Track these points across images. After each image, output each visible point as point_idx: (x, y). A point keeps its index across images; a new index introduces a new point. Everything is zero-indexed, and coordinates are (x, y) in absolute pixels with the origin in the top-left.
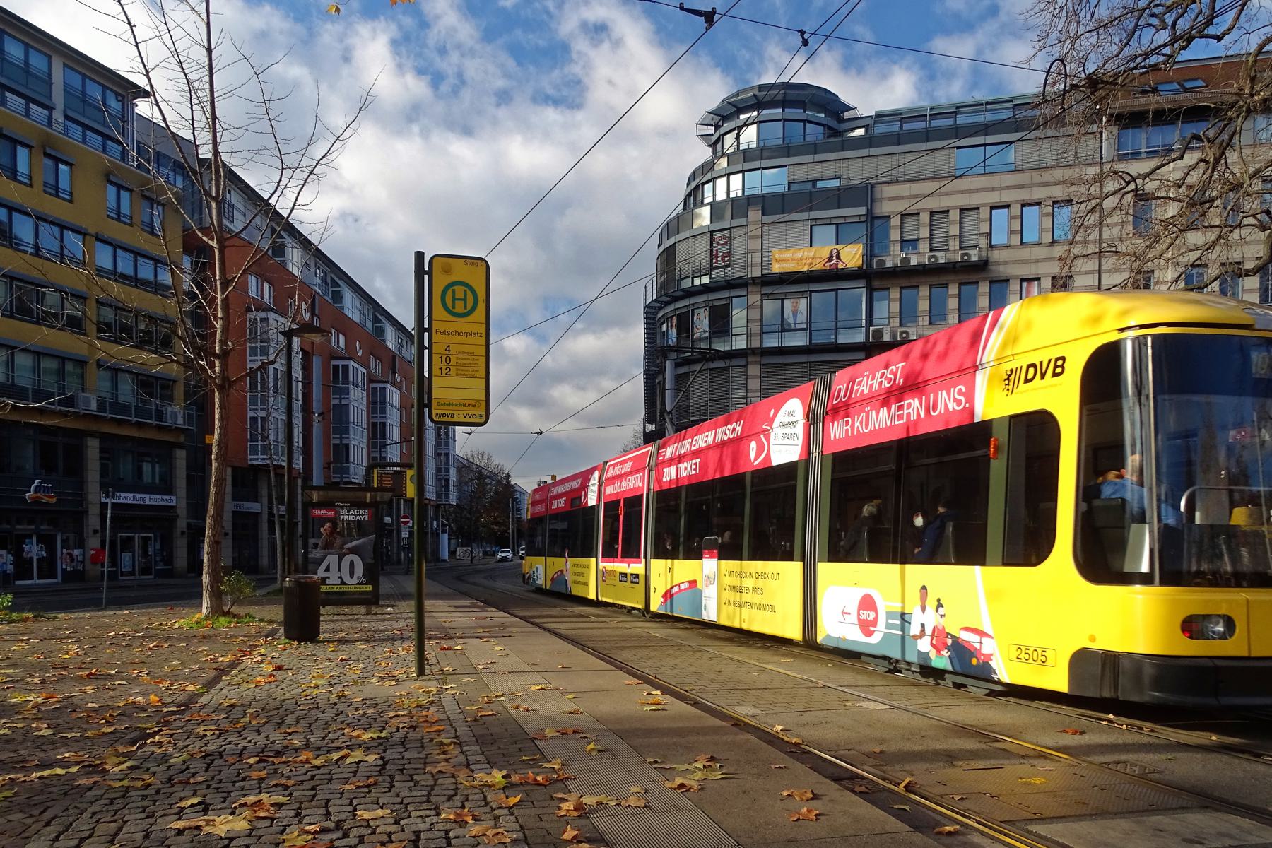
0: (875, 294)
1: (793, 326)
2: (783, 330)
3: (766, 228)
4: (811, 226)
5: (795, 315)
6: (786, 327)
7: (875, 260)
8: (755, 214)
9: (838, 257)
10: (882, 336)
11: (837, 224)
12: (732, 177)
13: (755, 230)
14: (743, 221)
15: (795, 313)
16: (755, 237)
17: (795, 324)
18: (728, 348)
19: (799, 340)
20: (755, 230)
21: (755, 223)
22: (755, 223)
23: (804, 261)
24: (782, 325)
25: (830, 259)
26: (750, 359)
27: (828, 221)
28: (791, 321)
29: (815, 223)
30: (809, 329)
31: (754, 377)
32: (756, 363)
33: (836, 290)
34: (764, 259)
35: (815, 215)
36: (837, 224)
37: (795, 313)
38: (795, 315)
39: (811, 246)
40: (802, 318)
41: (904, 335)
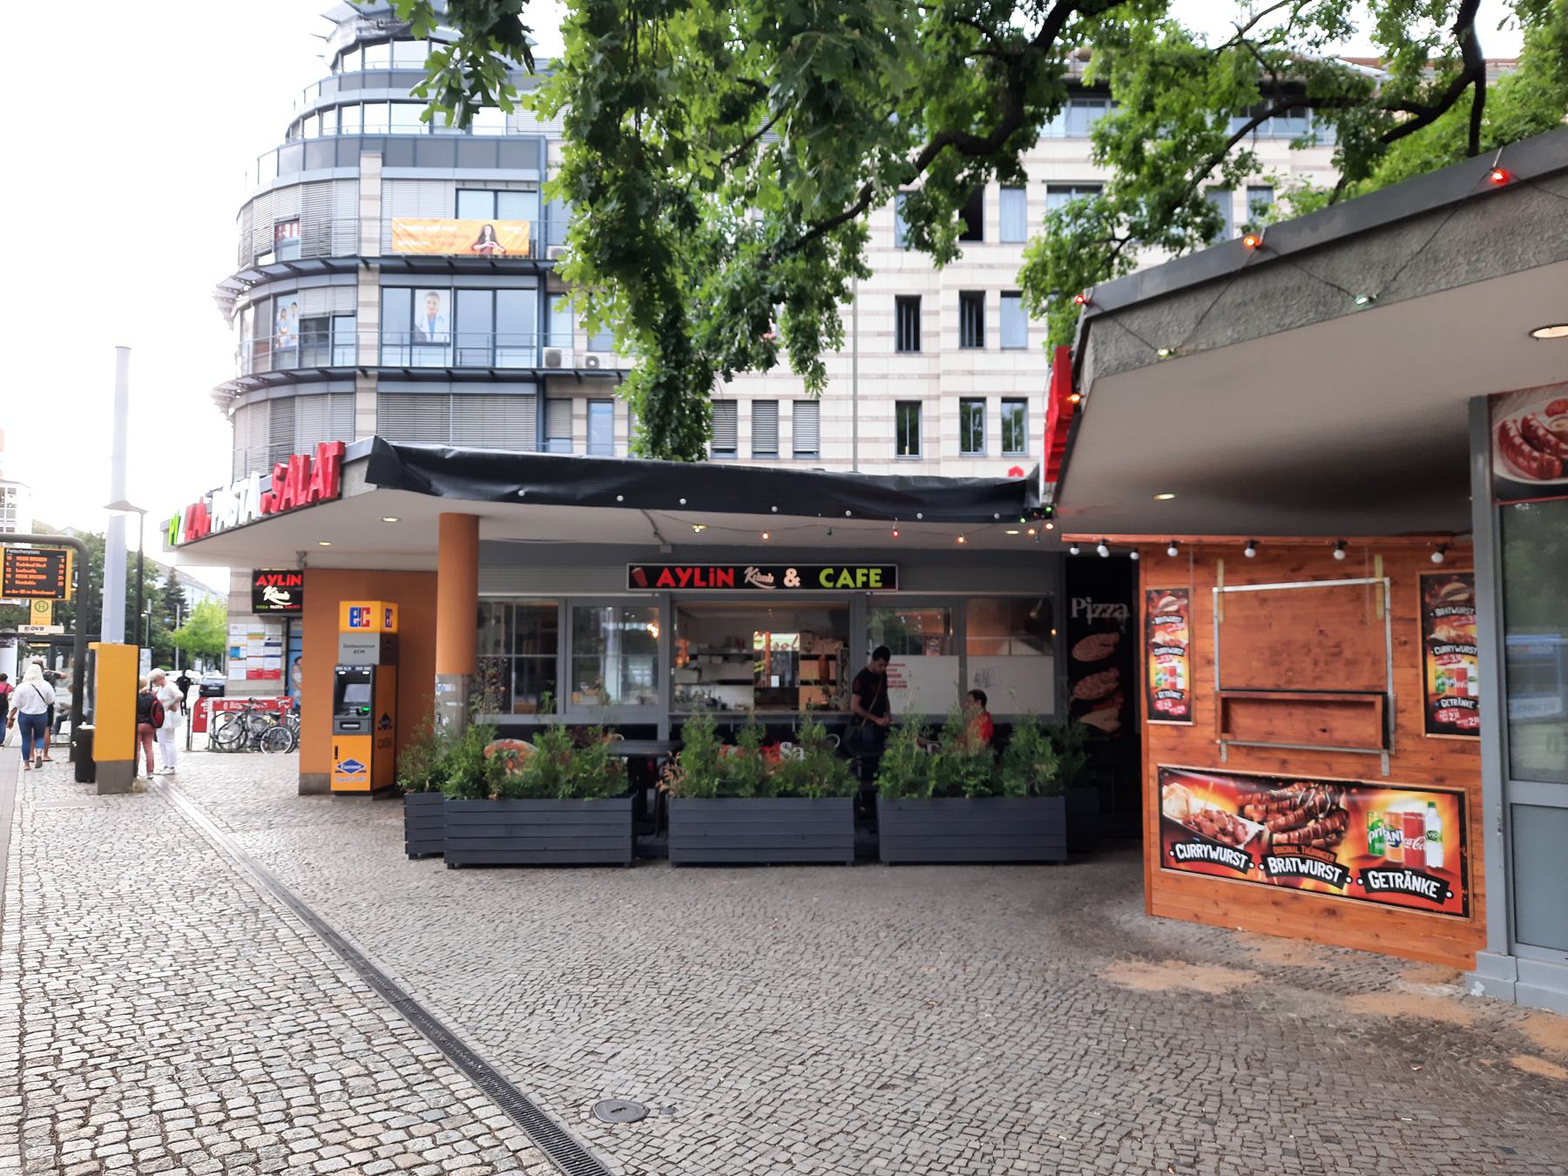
0: (555, 301)
1: (429, 339)
2: (412, 344)
3: (387, 185)
4: (458, 190)
5: (432, 324)
6: (419, 340)
7: (550, 248)
8: (371, 164)
9: (493, 238)
10: (559, 363)
11: (496, 192)
12: (345, 109)
13: (370, 186)
14: (350, 172)
15: (432, 319)
16: (371, 198)
17: (432, 333)
18: (324, 363)
19: (438, 360)
20: (370, 186)
21: (372, 177)
22: (372, 177)
23: (442, 239)
24: (412, 336)
25: (481, 239)
26: (361, 383)
27: (482, 186)
28: (425, 329)
29: (463, 186)
30: (453, 343)
31: (366, 412)
32: (370, 390)
33: (494, 289)
34: (385, 230)
35: (461, 173)
36: (496, 192)
37: (432, 319)
38: (432, 324)
39: (457, 217)
40: (442, 332)
41: (592, 363)
